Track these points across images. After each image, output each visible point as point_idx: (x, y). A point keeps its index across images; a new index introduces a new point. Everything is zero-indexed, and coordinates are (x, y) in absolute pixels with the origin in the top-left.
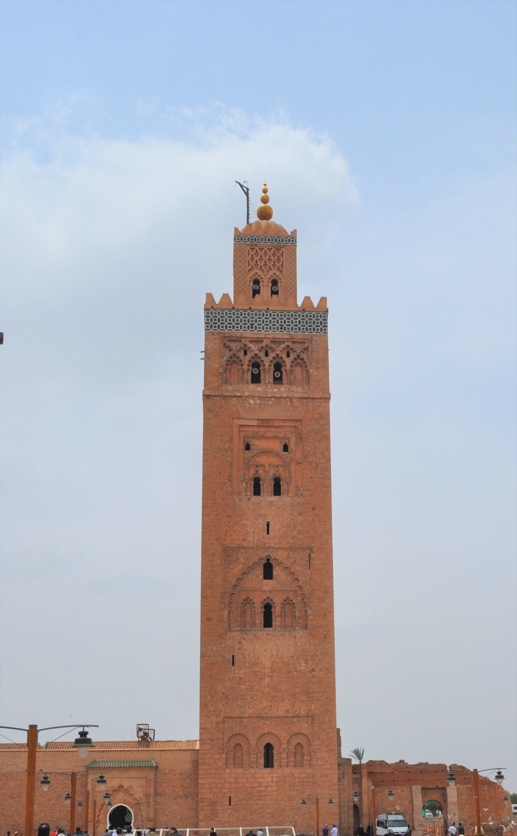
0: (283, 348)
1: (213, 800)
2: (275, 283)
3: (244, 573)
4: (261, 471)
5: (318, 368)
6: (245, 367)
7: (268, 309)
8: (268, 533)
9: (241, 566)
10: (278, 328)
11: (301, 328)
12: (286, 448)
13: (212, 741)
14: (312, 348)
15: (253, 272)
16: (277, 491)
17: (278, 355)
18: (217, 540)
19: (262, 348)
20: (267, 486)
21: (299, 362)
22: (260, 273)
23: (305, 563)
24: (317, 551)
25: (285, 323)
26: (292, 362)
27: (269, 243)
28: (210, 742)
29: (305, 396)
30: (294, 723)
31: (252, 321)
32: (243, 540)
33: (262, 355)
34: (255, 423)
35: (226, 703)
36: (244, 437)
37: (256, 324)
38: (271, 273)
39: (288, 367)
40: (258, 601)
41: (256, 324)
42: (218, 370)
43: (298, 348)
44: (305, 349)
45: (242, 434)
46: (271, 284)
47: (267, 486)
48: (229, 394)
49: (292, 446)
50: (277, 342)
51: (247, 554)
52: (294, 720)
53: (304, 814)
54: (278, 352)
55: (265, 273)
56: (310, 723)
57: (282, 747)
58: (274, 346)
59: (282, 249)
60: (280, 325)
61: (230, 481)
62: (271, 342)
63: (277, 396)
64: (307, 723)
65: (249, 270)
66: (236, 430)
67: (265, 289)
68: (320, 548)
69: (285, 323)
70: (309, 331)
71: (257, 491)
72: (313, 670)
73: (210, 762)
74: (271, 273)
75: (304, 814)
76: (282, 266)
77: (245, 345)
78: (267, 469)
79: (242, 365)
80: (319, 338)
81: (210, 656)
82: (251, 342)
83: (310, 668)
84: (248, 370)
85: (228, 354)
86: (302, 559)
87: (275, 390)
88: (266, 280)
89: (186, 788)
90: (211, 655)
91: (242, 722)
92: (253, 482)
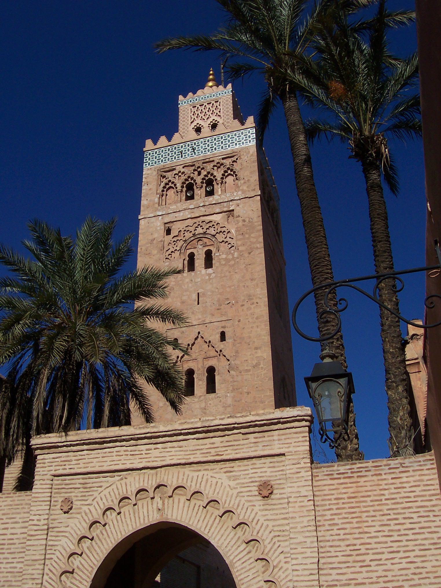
15: (195, 123)
17: (209, 173)
21: (230, 172)
26: (223, 175)
43: (227, 162)
44: (234, 161)
65: (192, 123)
76: (220, 112)
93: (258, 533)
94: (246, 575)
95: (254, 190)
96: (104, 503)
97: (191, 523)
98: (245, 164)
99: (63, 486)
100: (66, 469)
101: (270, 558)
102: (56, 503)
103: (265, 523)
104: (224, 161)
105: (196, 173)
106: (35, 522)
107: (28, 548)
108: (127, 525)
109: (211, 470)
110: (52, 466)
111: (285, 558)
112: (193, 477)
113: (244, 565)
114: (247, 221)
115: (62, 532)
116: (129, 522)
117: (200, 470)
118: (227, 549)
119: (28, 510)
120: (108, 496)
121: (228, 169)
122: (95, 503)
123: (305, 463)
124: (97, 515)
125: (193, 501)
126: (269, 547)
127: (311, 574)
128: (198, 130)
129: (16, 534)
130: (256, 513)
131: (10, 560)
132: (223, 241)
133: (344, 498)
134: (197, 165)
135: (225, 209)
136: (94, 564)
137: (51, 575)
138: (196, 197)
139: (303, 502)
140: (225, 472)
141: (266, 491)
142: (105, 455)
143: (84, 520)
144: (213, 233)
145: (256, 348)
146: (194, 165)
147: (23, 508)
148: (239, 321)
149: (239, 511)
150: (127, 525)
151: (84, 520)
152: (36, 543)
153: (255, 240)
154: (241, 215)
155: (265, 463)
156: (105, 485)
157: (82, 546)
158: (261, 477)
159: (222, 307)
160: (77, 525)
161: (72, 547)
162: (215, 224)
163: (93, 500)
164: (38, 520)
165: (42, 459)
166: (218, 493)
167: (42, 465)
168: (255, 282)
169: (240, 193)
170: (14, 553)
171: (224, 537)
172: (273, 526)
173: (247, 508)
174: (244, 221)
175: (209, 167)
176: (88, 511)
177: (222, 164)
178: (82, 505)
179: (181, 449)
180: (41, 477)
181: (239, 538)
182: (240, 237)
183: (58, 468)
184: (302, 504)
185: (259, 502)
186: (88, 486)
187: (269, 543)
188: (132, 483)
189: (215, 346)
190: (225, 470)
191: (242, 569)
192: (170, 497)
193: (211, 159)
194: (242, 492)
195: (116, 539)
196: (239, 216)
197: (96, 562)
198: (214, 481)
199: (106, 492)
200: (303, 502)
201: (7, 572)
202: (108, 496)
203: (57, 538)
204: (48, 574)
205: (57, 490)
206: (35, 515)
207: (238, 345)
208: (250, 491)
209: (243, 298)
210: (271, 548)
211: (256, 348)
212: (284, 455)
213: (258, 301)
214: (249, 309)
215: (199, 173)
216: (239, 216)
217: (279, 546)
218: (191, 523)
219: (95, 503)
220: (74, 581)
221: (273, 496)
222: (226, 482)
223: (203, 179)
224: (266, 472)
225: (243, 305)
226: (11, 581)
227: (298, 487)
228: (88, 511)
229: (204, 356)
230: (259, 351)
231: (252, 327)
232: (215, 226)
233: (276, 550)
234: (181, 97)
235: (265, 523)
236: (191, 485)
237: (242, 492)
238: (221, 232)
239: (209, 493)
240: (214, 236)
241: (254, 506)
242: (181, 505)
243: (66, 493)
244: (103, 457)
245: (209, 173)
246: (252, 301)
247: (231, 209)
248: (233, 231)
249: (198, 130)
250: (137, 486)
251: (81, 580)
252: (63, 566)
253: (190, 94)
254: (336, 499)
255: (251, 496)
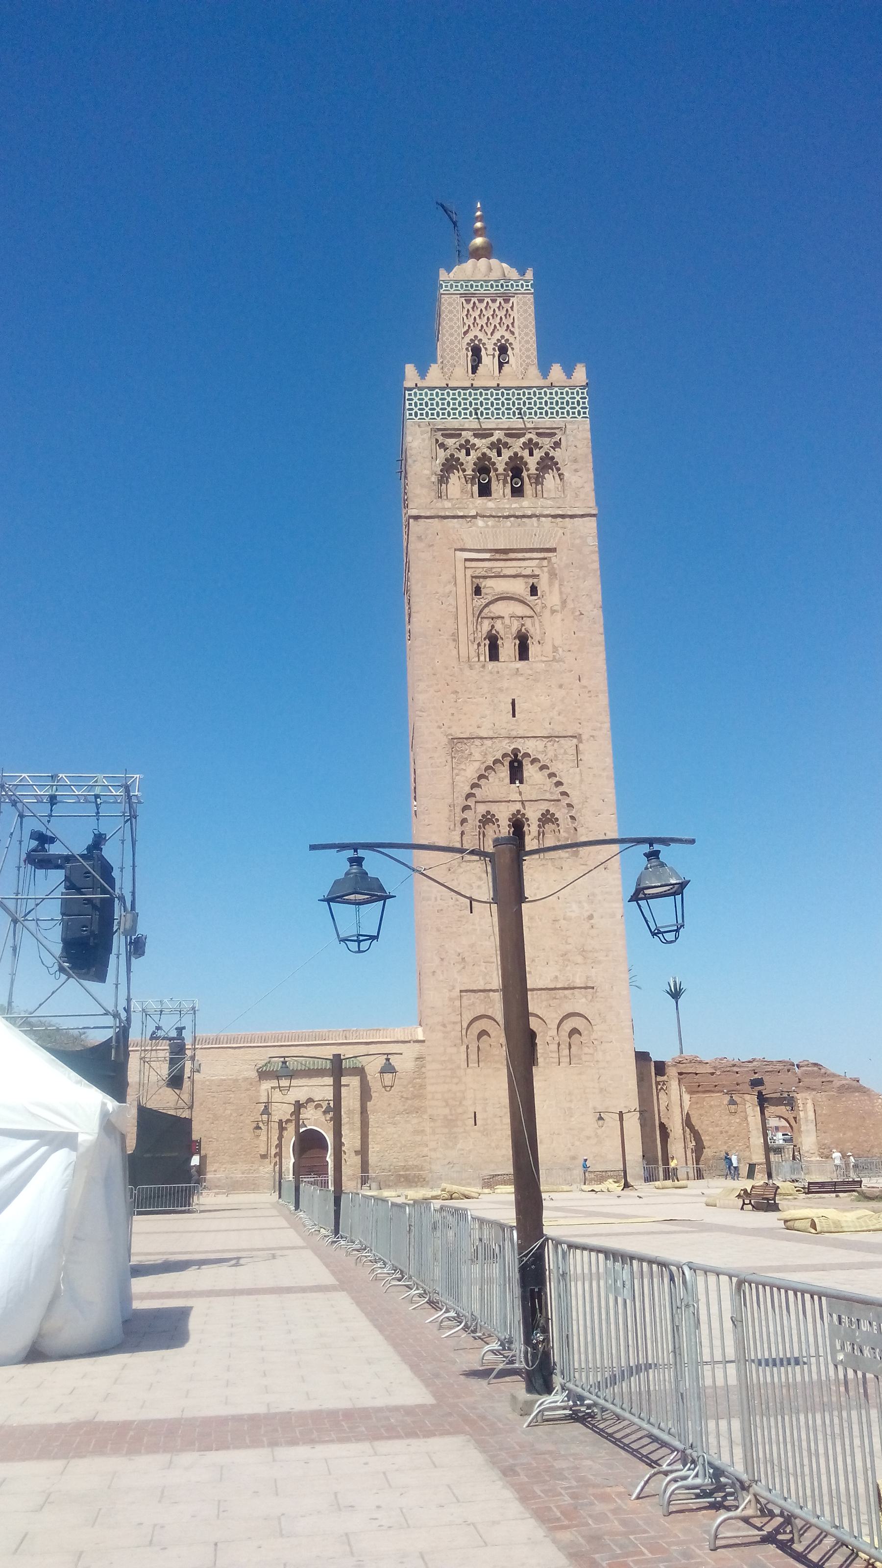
0: (524, 443)
1: (450, 1117)
2: (503, 350)
3: (481, 777)
4: (499, 625)
5: (576, 471)
6: (469, 472)
7: (498, 385)
8: (514, 716)
9: (477, 765)
10: (514, 412)
11: (549, 411)
12: (534, 590)
13: (444, 1026)
14: (567, 440)
15: (470, 336)
16: (523, 653)
18: (440, 727)
19: (492, 444)
20: (508, 648)
21: (548, 464)
22: (481, 335)
23: (571, 757)
24: (588, 740)
25: (524, 405)
27: (492, 291)
28: (442, 1028)
29: (561, 513)
30: (565, 997)
31: (476, 404)
32: (478, 727)
33: (493, 454)
34: (487, 556)
35: (464, 968)
36: (472, 577)
37: (482, 409)
38: (497, 335)
39: (533, 470)
40: (504, 814)
41: (482, 409)
42: (429, 478)
43: (546, 442)
44: (555, 443)
45: (469, 573)
46: (497, 353)
47: (508, 648)
48: (447, 514)
49: (543, 585)
50: (514, 434)
51: (484, 748)
52: (566, 992)
53: (588, 1138)
54: (518, 450)
55: (489, 336)
56: (590, 997)
57: (550, 1033)
58: (509, 440)
59: (512, 299)
60: (517, 409)
61: (454, 640)
62: (506, 435)
63: (517, 514)
64: (586, 997)
65: (465, 333)
66: (460, 566)
67: (489, 361)
68: (593, 736)
69: (524, 405)
70: (560, 415)
71: (494, 655)
72: (591, 917)
73: (443, 1058)
74: (497, 335)
75: (588, 1138)
77: (467, 441)
78: (507, 621)
79: (464, 471)
80: (576, 426)
81: (436, 899)
82: (476, 436)
83: (586, 914)
84: (473, 478)
85: (442, 455)
86: (565, 753)
87: (514, 506)
88: (490, 347)
89: (407, 1099)
90: (438, 899)
91: (489, 997)
92: (487, 642)
104: (540, 440)
175: (517, 445)
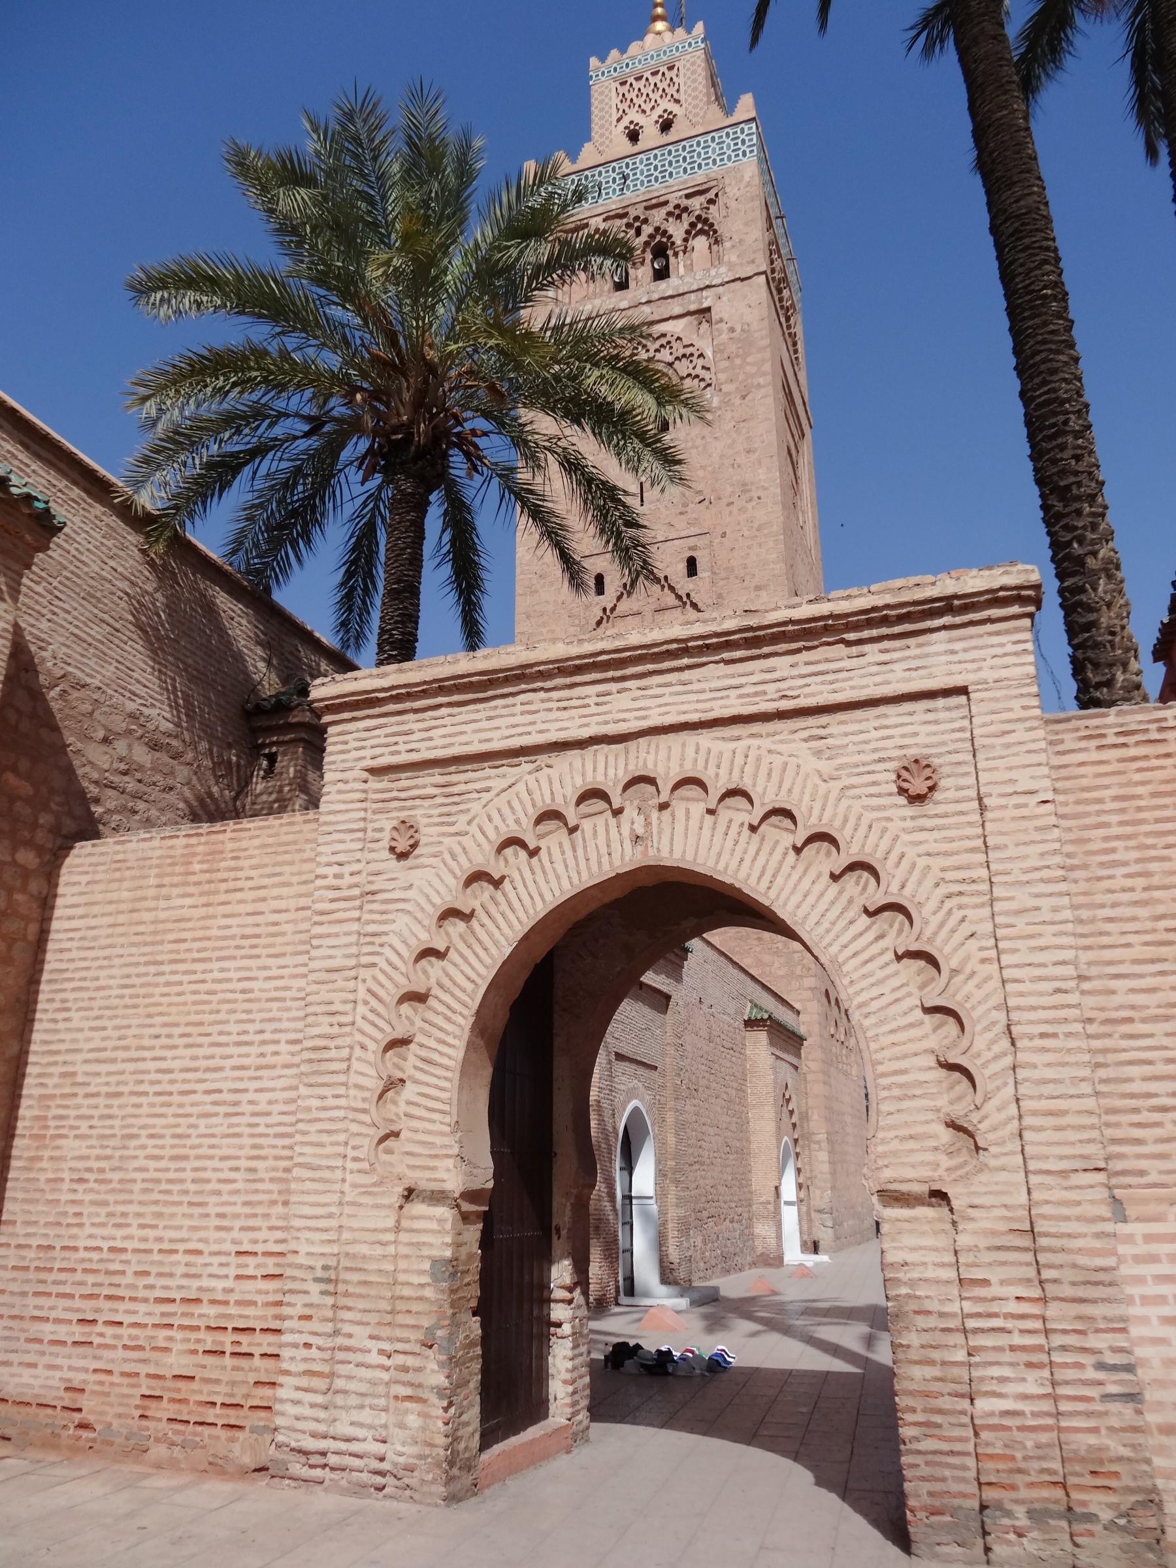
17: (657, 229)
26: (688, 232)
38: (659, 111)
43: (696, 203)
44: (711, 202)
65: (619, 120)
93: (903, 887)
94: (875, 992)
95: (753, 262)
96: (496, 828)
97: (721, 867)
98: (733, 204)
99: (395, 794)
100: (398, 753)
101: (941, 951)
102: (377, 835)
103: (922, 862)
105: (632, 232)
106: (331, 881)
107: (315, 942)
108: (558, 877)
109: (768, 735)
110: (363, 748)
111: (981, 949)
112: (721, 753)
113: (870, 967)
114: (739, 330)
115: (398, 900)
116: (560, 868)
117: (738, 739)
118: (821, 930)
119: (313, 854)
120: (506, 811)
121: (699, 217)
122: (474, 829)
123: (1024, 708)
124: (482, 857)
125: (724, 815)
126: (935, 920)
127: (1058, 991)
128: (634, 136)
129: (287, 911)
130: (896, 839)
131: (275, 972)
132: (689, 375)
133: (1140, 797)
134: (633, 213)
135: (693, 307)
136: (479, 975)
137: (374, 1003)
138: (632, 284)
139: (1026, 805)
140: (805, 740)
141: (916, 786)
142: (492, 713)
143: (451, 871)
144: (670, 359)
145: (758, 588)
146: (625, 215)
147: (300, 851)
148: (724, 535)
149: (848, 832)
150: (558, 877)
151: (451, 871)
152: (335, 929)
153: (753, 370)
154: (726, 317)
155: (911, 714)
156: (497, 784)
157: (447, 934)
158: (901, 747)
159: (688, 509)
160: (433, 882)
161: (424, 936)
162: (673, 340)
163: (469, 823)
164: (336, 876)
165: (339, 734)
166: (790, 791)
167: (340, 747)
168: (753, 457)
169: (723, 270)
170: (283, 955)
171: (811, 899)
172: (943, 870)
173: (870, 827)
174: (732, 330)
175: (658, 216)
176: (458, 849)
177: (686, 209)
178: (444, 834)
179: (689, 687)
180: (340, 776)
181: (851, 901)
182: (726, 364)
183: (378, 751)
184: (1024, 812)
185: (901, 809)
186: (455, 789)
187: (935, 913)
188: (563, 778)
189: (677, 587)
190: (805, 734)
191: (864, 976)
192: (663, 807)
193: (662, 199)
194: (853, 787)
195: (531, 911)
196: (721, 321)
197: (483, 971)
198: (778, 761)
199: (501, 801)
200: (1026, 805)
201: (269, 1000)
202: (506, 811)
203: (385, 917)
204: (366, 1003)
205: (380, 805)
206: (329, 864)
207: (721, 583)
208: (874, 783)
209: (730, 489)
210: (942, 924)
211: (758, 588)
212: (963, 691)
213: (760, 493)
214: (742, 510)
215: (638, 232)
216: (721, 321)
217: (963, 920)
218: (721, 867)
219: (474, 829)
220: (430, 1016)
221: (937, 795)
222: (811, 764)
223: (647, 244)
224: (916, 734)
225: (730, 504)
226: (280, 1020)
227: (1010, 768)
228: (458, 849)
229: (655, 606)
230: (763, 593)
231: (749, 547)
232: (673, 344)
233: (953, 931)
234: (594, 62)
235: (922, 862)
236: (717, 775)
237: (853, 787)
238: (684, 356)
239: (767, 796)
240: (671, 365)
241: (889, 819)
242: (694, 823)
243: (403, 809)
244: (489, 718)
245: (657, 229)
246: (748, 495)
247: (705, 305)
248: (709, 353)
249: (634, 136)
250: (579, 782)
251: (449, 1013)
252: (402, 980)
253: (614, 53)
254: (1116, 798)
255: (879, 795)
